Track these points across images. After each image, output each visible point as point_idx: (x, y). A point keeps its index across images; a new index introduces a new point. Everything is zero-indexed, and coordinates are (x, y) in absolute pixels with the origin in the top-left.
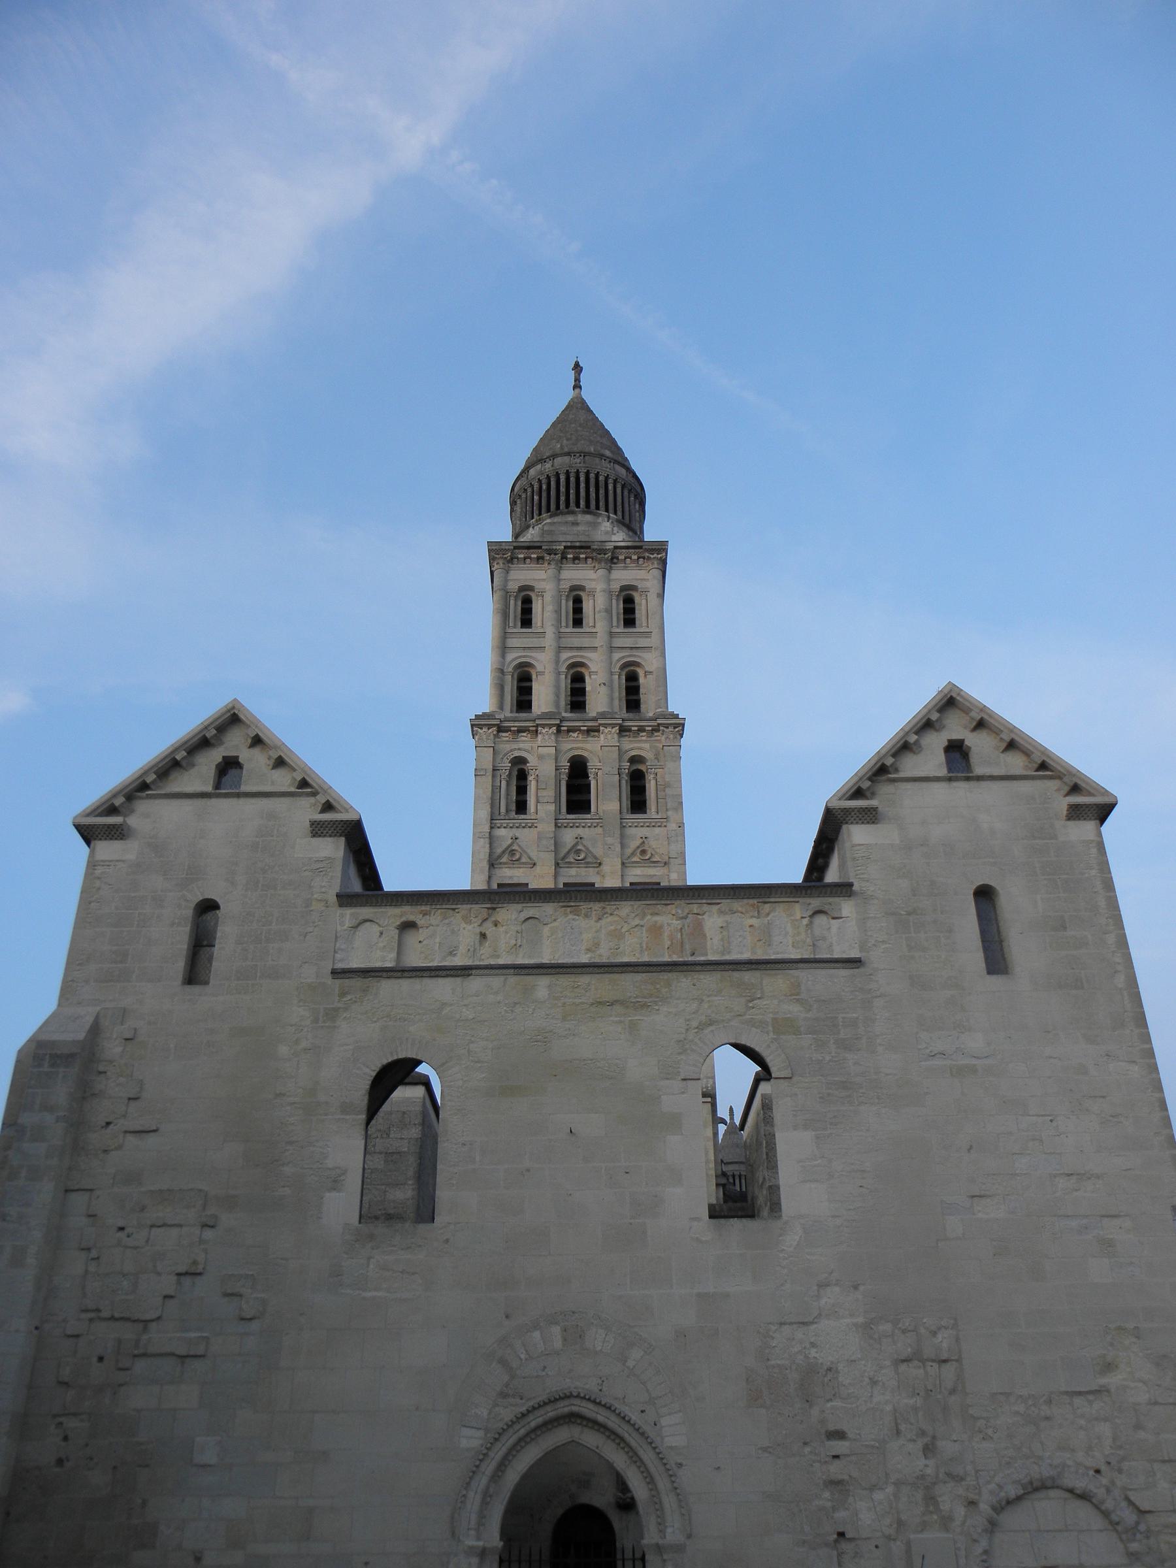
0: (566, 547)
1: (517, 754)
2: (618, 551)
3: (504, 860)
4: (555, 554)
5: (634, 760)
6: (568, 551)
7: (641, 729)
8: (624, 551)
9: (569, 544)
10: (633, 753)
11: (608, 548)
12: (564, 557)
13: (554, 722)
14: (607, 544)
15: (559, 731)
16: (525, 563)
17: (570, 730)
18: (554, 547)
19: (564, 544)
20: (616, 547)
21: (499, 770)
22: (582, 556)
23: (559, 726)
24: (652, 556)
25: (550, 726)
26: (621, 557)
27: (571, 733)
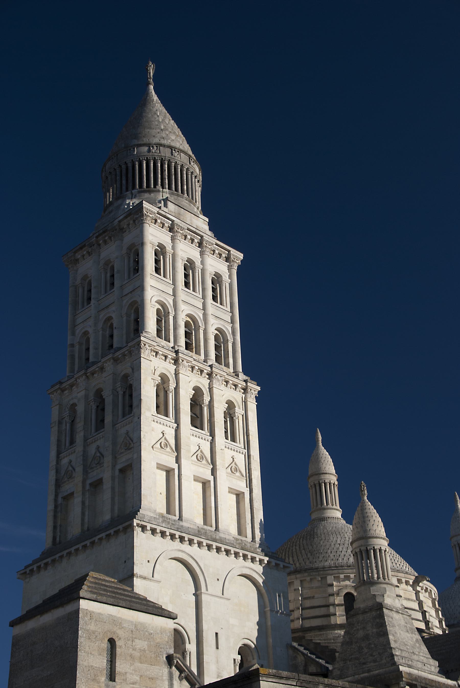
0: (97, 237)
1: (71, 402)
2: (122, 223)
3: (66, 479)
4: (94, 245)
5: (126, 377)
6: (99, 238)
7: (124, 355)
8: (125, 221)
9: (97, 234)
10: (123, 373)
11: (115, 225)
12: (99, 245)
13: (82, 373)
14: (115, 222)
15: (87, 377)
16: (84, 259)
17: (93, 374)
18: (91, 241)
19: (95, 235)
20: (120, 222)
21: (64, 418)
22: (107, 238)
23: (85, 374)
24: (137, 216)
25: (81, 376)
26: (125, 226)
27: (95, 375)
